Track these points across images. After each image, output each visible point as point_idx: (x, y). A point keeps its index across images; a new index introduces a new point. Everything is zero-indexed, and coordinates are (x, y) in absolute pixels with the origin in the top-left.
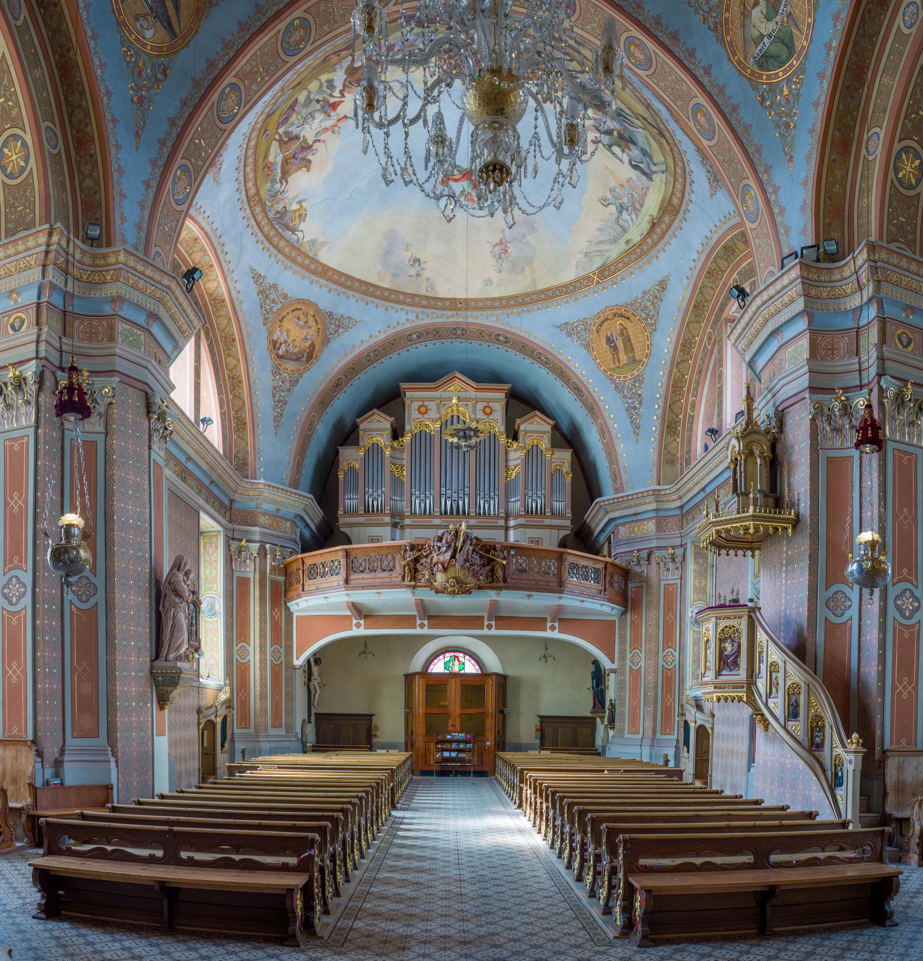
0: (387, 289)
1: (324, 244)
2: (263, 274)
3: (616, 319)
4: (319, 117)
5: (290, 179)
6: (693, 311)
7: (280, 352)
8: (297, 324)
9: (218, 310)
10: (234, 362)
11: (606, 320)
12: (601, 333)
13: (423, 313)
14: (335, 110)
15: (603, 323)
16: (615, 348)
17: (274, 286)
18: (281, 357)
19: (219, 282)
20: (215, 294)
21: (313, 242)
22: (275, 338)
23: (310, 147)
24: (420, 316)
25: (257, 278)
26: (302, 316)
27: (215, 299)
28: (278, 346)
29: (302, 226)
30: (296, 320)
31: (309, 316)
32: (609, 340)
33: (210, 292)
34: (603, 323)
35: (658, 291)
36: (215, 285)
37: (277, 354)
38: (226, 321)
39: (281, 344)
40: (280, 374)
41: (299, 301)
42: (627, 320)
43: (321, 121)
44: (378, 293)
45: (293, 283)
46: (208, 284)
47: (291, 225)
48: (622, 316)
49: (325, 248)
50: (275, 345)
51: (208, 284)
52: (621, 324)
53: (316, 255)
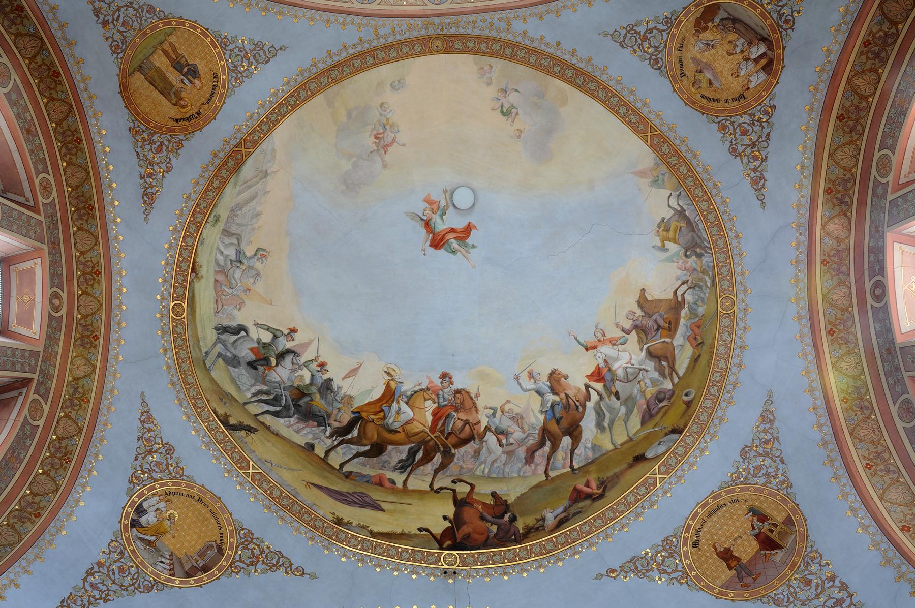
0: (555, 75)
1: (642, 174)
2: (747, 183)
3: (195, 110)
4: (618, 367)
5: (670, 296)
6: (91, 198)
7: (762, 49)
8: (715, 75)
9: (845, 181)
10: (858, 82)
11: (210, 100)
12: (210, 76)
13: (499, 31)
14: (598, 368)
15: (213, 93)
16: (178, 65)
17: (735, 153)
18: (764, 39)
19: (823, 227)
20: (837, 209)
21: (656, 183)
22: (762, 76)
23: (636, 327)
24: (503, 25)
25: (758, 183)
26: (704, 85)
27: (841, 202)
28: (764, 62)
29: (668, 214)
30: (716, 84)
31: (692, 79)
32: (193, 73)
33: (843, 220)
34: (213, 93)
35: (151, 186)
36: (831, 227)
37: (770, 47)
38: (840, 155)
39: (756, 61)
40: (780, 15)
41: (703, 111)
42: (179, 116)
43: (617, 360)
44: (569, 73)
45: (705, 143)
46: (842, 234)
47: (683, 224)
48: (188, 119)
49: (641, 167)
50: (770, 65)
51: (842, 234)
52: (183, 107)
53: (656, 164)
